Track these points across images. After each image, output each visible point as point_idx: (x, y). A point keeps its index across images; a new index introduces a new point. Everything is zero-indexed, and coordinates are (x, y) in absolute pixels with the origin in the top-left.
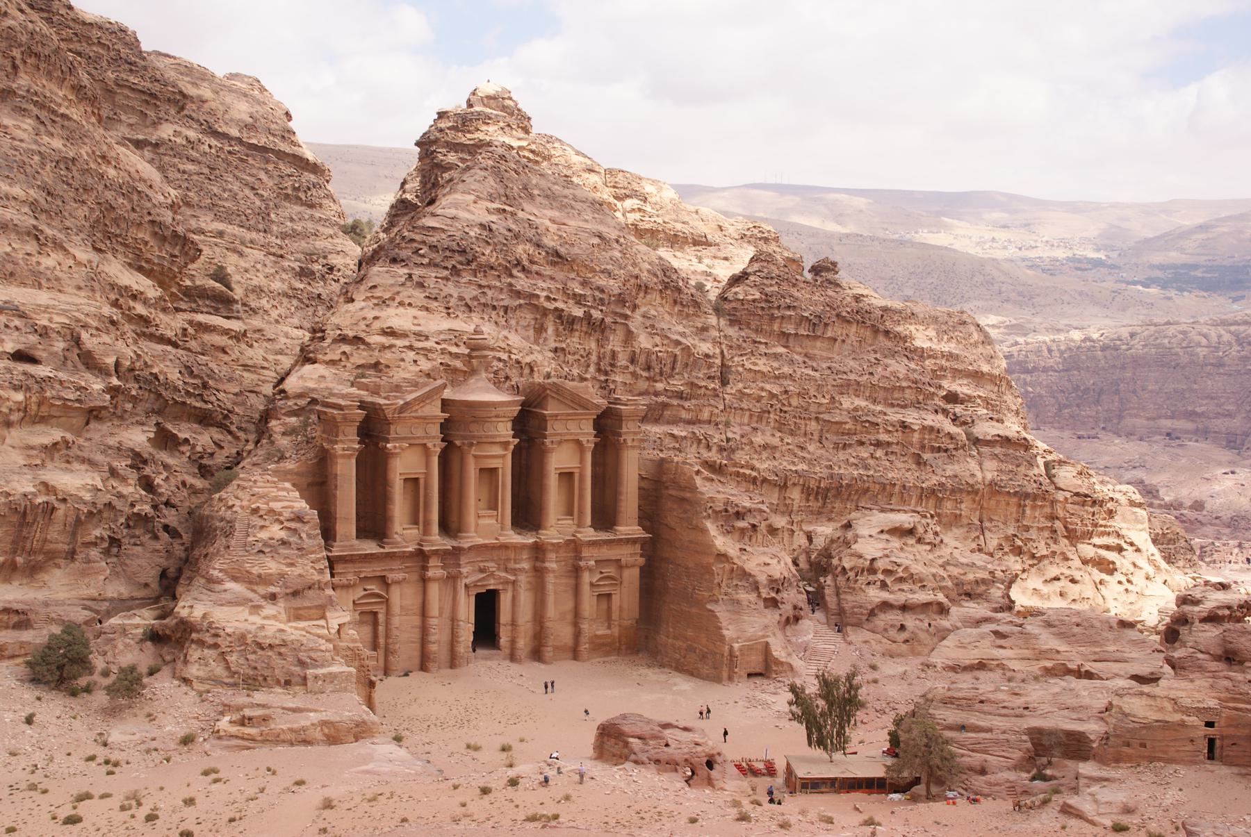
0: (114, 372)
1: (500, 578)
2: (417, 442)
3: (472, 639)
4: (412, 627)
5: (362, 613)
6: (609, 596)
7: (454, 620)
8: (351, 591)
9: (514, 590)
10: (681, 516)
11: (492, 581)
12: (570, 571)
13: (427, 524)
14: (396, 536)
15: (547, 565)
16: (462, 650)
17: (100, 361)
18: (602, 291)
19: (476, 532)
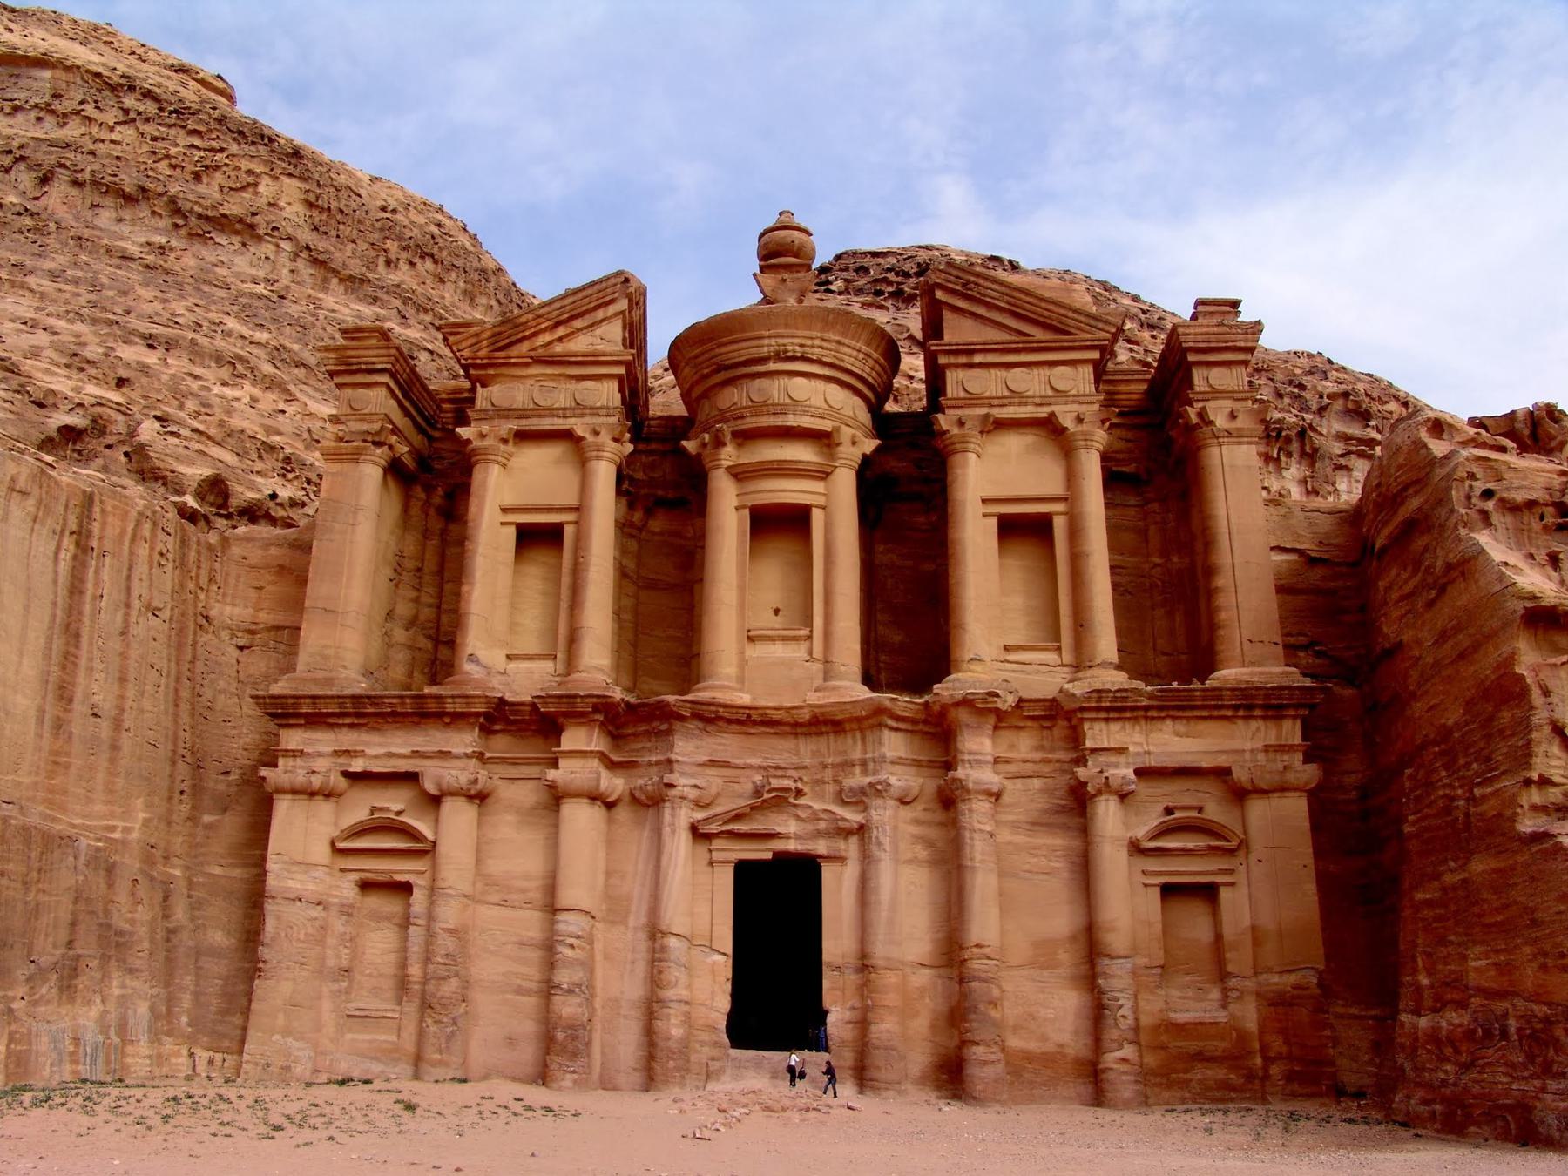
0: (192, 489)
1: (815, 817)
2: (547, 424)
3: (723, 1003)
4: (521, 944)
5: (366, 886)
6: (1207, 893)
7: (655, 933)
8: (324, 808)
9: (866, 859)
10: (1408, 588)
11: (792, 827)
12: (1061, 810)
13: (573, 639)
14: (468, 667)
15: (961, 773)
16: (677, 1032)
17: (162, 465)
18: (1301, 387)
19: (741, 679)
